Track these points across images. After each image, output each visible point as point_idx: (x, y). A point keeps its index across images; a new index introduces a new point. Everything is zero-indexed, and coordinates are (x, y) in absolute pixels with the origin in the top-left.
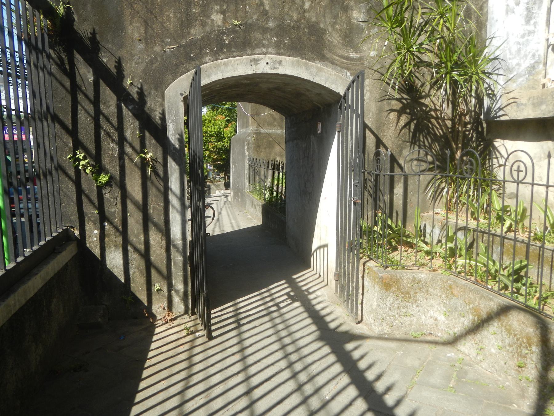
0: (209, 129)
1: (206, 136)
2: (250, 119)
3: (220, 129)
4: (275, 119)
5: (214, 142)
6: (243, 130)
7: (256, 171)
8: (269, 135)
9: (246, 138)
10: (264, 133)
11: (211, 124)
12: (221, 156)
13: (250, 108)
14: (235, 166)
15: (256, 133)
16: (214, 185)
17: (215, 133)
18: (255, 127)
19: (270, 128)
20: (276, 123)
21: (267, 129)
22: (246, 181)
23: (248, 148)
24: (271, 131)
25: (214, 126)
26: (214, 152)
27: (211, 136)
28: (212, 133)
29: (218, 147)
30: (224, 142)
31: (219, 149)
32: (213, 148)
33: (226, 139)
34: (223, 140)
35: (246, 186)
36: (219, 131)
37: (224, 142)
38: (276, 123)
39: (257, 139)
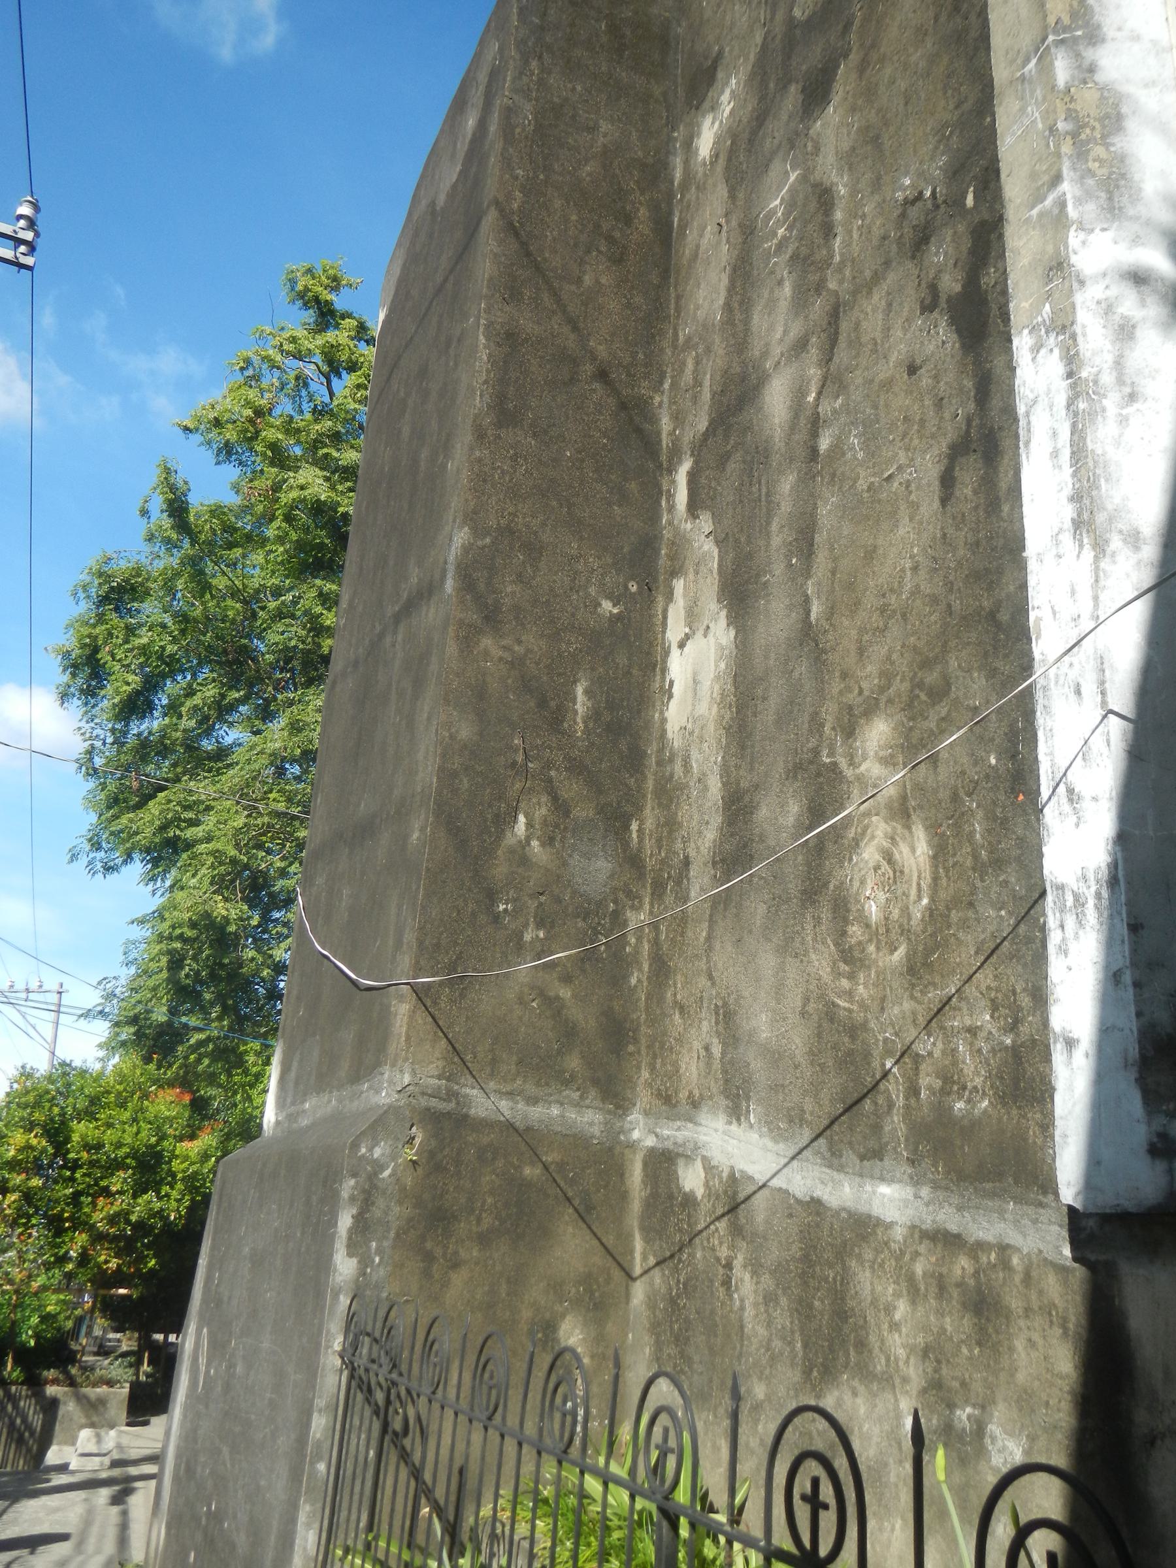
0: (110, 1136)
1: (92, 1164)
2: (402, 1010)
3: (162, 1137)
4: (569, 1033)
5: (121, 1192)
6: (316, 1107)
9: (355, 1146)
11: (126, 1115)
12: (142, 1259)
13: (410, 937)
14: (218, 1346)
15: (433, 1119)
16: (81, 1399)
17: (134, 1154)
18: (433, 1069)
19: (531, 1089)
20: (574, 1062)
21: (510, 1094)
22: (305, 1512)
23: (362, 1226)
24: (536, 1113)
25: (135, 1120)
26: (115, 1239)
27: (116, 1165)
28: (121, 1153)
29: (133, 1218)
30: (167, 1195)
32: (112, 1220)
33: (179, 1186)
34: (165, 1189)
37: (167, 1195)
38: (574, 1062)
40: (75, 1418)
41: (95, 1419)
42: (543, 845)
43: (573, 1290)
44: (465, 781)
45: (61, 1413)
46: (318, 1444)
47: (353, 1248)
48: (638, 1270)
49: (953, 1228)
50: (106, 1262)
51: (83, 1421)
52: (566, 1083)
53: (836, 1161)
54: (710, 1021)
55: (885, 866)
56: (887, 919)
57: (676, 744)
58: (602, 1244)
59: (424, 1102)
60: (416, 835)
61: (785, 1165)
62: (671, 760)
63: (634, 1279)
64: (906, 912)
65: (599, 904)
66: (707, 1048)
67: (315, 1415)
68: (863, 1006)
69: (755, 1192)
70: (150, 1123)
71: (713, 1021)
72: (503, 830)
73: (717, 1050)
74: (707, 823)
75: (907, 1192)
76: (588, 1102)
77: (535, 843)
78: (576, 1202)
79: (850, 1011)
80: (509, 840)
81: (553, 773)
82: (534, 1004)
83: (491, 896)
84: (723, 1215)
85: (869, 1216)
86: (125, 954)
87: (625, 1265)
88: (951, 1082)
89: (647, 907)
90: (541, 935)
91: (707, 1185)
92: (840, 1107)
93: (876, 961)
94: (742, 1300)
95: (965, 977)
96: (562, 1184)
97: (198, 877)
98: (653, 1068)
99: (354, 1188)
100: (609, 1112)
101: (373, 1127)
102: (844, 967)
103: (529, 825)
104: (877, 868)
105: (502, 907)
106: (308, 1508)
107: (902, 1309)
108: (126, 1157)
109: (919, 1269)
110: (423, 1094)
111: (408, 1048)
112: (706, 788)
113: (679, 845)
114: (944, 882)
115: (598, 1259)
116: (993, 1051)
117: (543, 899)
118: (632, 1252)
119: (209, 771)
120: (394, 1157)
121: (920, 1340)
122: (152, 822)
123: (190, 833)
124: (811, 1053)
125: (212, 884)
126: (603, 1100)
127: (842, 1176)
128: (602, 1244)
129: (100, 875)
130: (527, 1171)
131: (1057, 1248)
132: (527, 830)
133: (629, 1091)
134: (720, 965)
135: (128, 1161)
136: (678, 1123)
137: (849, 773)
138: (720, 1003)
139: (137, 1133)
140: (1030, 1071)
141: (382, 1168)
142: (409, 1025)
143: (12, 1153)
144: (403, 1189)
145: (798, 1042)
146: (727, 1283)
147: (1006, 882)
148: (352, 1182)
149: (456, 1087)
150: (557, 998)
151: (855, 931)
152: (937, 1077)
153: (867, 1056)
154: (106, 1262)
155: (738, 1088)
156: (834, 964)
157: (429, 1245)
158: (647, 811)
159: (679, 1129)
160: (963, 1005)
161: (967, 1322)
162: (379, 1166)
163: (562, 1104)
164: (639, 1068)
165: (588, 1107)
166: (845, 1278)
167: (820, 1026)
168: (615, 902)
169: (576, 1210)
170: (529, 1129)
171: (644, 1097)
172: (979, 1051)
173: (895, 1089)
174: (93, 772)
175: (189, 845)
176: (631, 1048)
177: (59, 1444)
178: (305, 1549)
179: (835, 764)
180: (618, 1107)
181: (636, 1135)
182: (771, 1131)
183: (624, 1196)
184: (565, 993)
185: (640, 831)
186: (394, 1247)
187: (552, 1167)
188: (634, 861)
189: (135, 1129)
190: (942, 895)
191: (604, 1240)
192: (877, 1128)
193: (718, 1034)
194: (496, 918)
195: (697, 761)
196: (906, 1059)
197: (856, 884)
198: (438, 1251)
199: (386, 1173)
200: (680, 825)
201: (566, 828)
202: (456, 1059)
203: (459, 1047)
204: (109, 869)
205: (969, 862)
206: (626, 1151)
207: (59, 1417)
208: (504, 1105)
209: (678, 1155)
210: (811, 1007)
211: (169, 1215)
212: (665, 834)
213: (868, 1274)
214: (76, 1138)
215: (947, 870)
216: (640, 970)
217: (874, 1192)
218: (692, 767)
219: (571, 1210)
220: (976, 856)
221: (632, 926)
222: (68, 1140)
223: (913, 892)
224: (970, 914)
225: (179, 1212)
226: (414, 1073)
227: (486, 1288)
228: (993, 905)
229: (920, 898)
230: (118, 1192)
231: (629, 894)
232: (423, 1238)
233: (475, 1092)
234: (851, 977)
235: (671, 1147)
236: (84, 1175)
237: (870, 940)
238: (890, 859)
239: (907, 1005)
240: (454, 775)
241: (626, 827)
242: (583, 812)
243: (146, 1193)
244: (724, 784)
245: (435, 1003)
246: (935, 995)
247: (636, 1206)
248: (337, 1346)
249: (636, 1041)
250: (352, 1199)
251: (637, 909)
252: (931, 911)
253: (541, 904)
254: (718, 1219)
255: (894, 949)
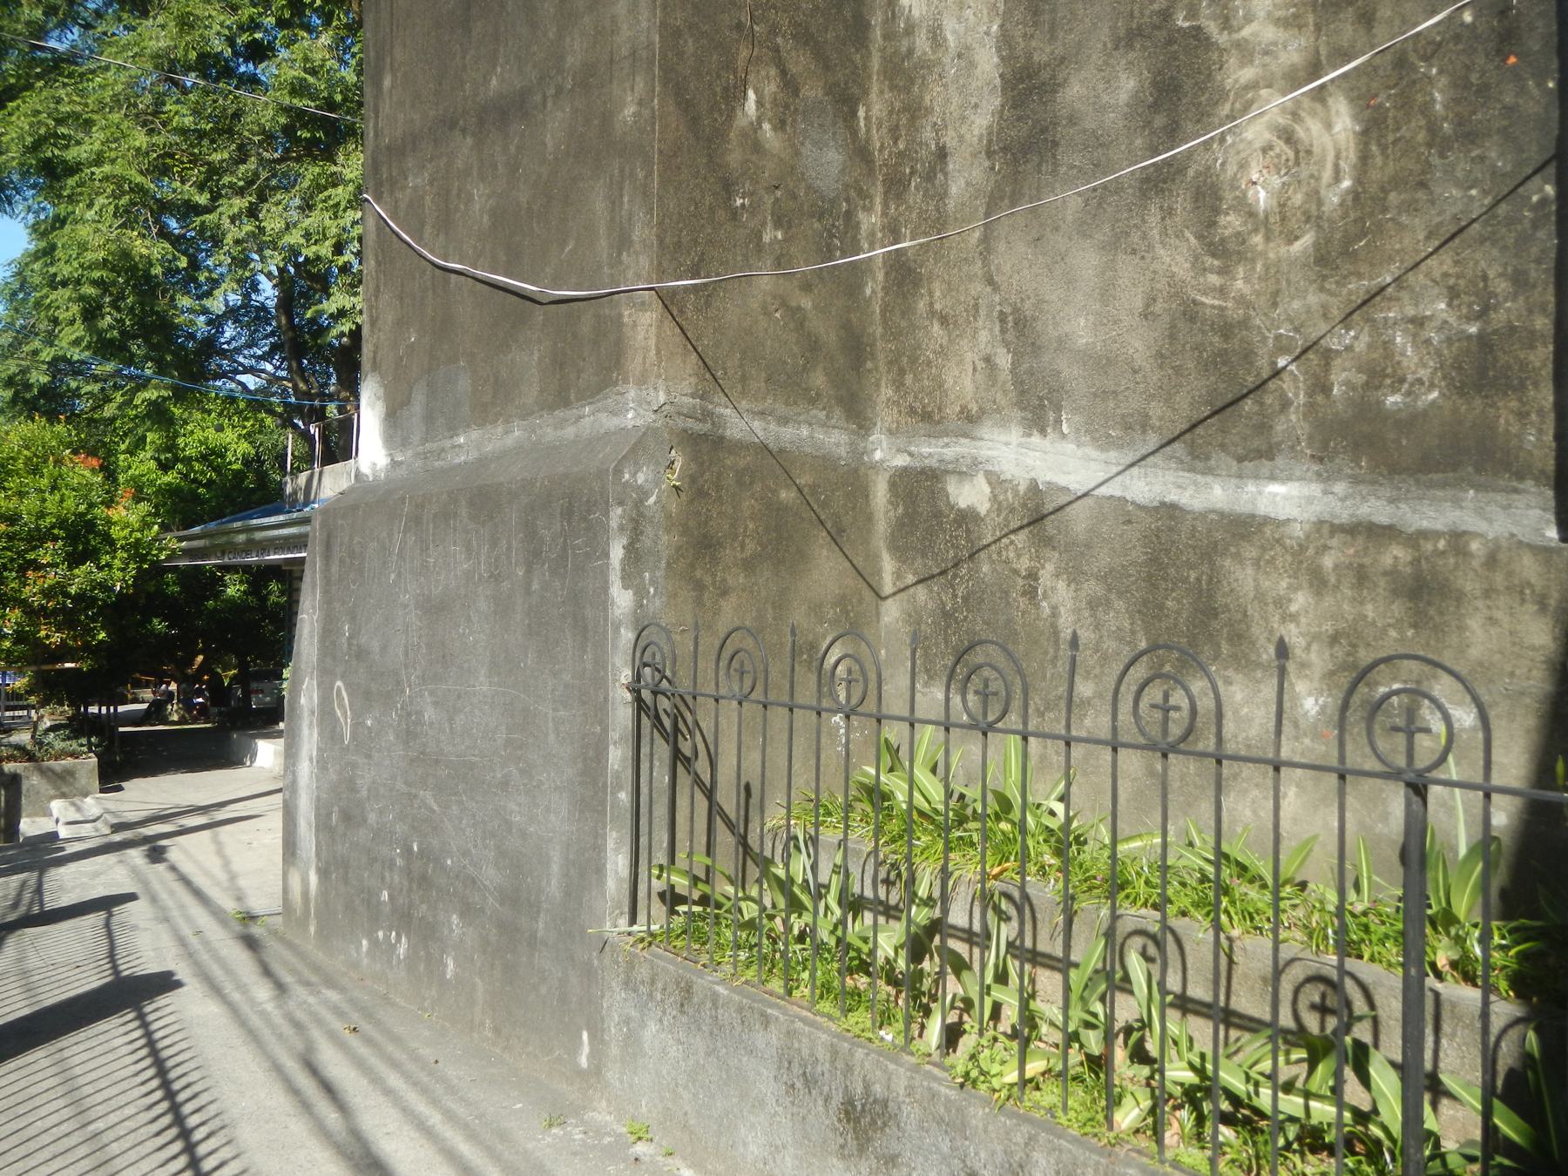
0: (29, 505)
3: (91, 505)
4: (813, 346)
5: (54, 565)
7: (686, 748)
8: (777, 460)
9: (618, 472)
10: (738, 447)
11: (44, 482)
12: (90, 632)
16: (43, 772)
17: (62, 523)
19: (781, 409)
20: (819, 379)
25: (54, 488)
26: (55, 612)
27: (38, 538)
28: (49, 520)
29: (73, 590)
30: (109, 565)
31: (79, 598)
32: (47, 593)
33: (120, 554)
34: (105, 559)
35: (611, 884)
36: (82, 515)
37: (109, 565)
39: (696, 490)
40: (42, 791)
41: (65, 789)
42: (774, 129)
43: (832, 612)
44: (690, 42)
45: (24, 788)
46: (617, 775)
47: (627, 579)
48: (888, 588)
49: (1383, 519)
50: (48, 637)
51: (52, 792)
52: (813, 401)
53: (1199, 465)
54: (991, 330)
55: (1280, 146)
56: (1282, 205)
57: (916, 13)
58: (853, 565)
59: (681, 423)
60: (629, 111)
61: (1119, 473)
62: (910, 30)
63: (884, 599)
64: (1315, 196)
65: (833, 202)
66: (987, 359)
67: (611, 747)
68: (1241, 301)
69: (1070, 503)
70: (74, 490)
71: (997, 329)
72: (733, 109)
73: (1004, 360)
74: (976, 106)
75: (1315, 489)
76: (834, 421)
77: (766, 126)
78: (829, 525)
79: (1222, 309)
80: (741, 122)
81: (779, 40)
82: (778, 315)
83: (728, 187)
84: (1021, 528)
85: (1253, 516)
87: (874, 585)
88: (1381, 372)
89: (878, 208)
90: (780, 236)
91: (994, 498)
92: (1206, 411)
93: (1264, 254)
94: (1054, 608)
95: (1409, 263)
96: (815, 507)
97: (96, 208)
98: (899, 385)
99: (622, 517)
100: (853, 432)
101: (633, 450)
102: (1210, 261)
103: (760, 103)
104: (1265, 150)
105: (739, 202)
106: (614, 834)
107: (1301, 601)
108: (53, 527)
109: (1328, 562)
110: (679, 414)
111: (660, 363)
112: (972, 65)
113: (928, 134)
114: (1379, 160)
115: (851, 581)
116: (1449, 341)
117: (779, 193)
118: (879, 572)
119: (70, 76)
120: (657, 484)
121: (1328, 627)
122: (21, 138)
123: (72, 154)
124: (1160, 355)
125: (115, 215)
126: (848, 418)
127: (1209, 479)
128: (853, 565)
130: (783, 495)
131: (1539, 531)
132: (757, 110)
133: (869, 410)
134: (1007, 268)
135: (56, 531)
136: (946, 440)
137: (1222, 39)
138: (1008, 310)
139: (62, 501)
140: (1503, 359)
141: (647, 495)
142: (658, 336)
144: (669, 517)
145: (1139, 345)
146: (1031, 593)
147: (1482, 159)
148: (619, 511)
149: (710, 407)
150: (799, 308)
151: (1231, 222)
152: (1360, 370)
153: (1248, 356)
154: (48, 637)
155: (1041, 399)
156: (1196, 258)
157: (698, 574)
158: (873, 96)
159: (947, 445)
160: (1405, 295)
161: (1398, 608)
162: (644, 494)
163: (810, 425)
164: (878, 385)
165: (834, 427)
166: (1214, 579)
167: (1173, 326)
168: (848, 200)
169: (829, 533)
170: (781, 451)
171: (885, 415)
172: (1428, 342)
173: (1295, 387)
175: (73, 169)
176: (869, 365)
177: (29, 816)
178: (617, 872)
179: (1199, 28)
180: (860, 427)
181: (878, 455)
182: (1093, 439)
183: (870, 518)
184: (807, 303)
185: (867, 118)
186: (666, 577)
187: (806, 490)
188: (861, 153)
189: (57, 497)
190: (1375, 175)
191: (855, 562)
192: (1263, 428)
193: (1006, 344)
194: (734, 214)
195: (954, 32)
196: (1311, 355)
197: (1231, 169)
198: (708, 580)
199: (652, 500)
200: (929, 111)
201: (796, 110)
202: (708, 376)
203: (710, 363)
205: (1421, 136)
206: (870, 472)
207: (24, 792)
208: (757, 425)
209: (947, 472)
210: (1158, 307)
211: (114, 585)
212: (904, 121)
213: (1250, 571)
215: (1383, 149)
216: (874, 279)
217: (1260, 493)
218: (945, 40)
219: (824, 534)
220: (1433, 129)
221: (864, 227)
223: (1327, 175)
224: (1421, 195)
225: (126, 582)
226: (668, 392)
227: (754, 614)
228: (1458, 184)
229: (1337, 178)
230: (49, 565)
231: (860, 192)
232: (692, 566)
233: (728, 411)
234: (1222, 272)
235: (935, 464)
237: (1256, 230)
238: (1288, 137)
239: (1313, 299)
240: (677, 33)
241: (854, 113)
242: (812, 91)
243: (84, 564)
244: (1002, 59)
245: (681, 312)
246: (1357, 287)
247: (882, 527)
248: (626, 675)
249: (873, 357)
250: (621, 528)
251: (868, 209)
252: (1356, 195)
253: (777, 200)
254: (1014, 531)
255: (1292, 238)
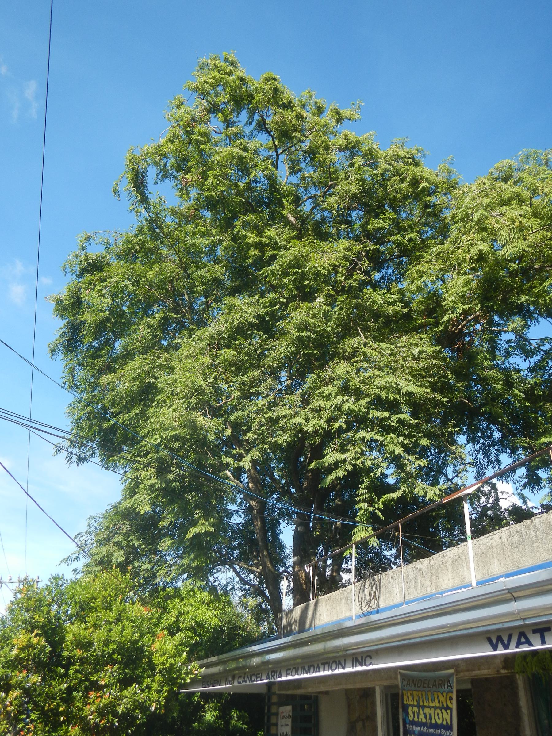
0: (99, 636)
1: (82, 661)
11: (113, 616)
17: (121, 648)
28: (112, 646)
29: (120, 709)
30: (149, 687)
32: (101, 712)
33: (158, 678)
36: (136, 642)
37: (149, 687)
70: (132, 621)
86: (89, 525)
108: (113, 653)
129: (75, 464)
135: (115, 656)
139: (123, 630)
143: (15, 652)
174: (74, 386)
189: (120, 628)
204: (81, 460)
211: (150, 706)
214: (69, 637)
222: (63, 639)
225: (159, 703)
230: (106, 686)
236: (77, 671)
243: (131, 686)
